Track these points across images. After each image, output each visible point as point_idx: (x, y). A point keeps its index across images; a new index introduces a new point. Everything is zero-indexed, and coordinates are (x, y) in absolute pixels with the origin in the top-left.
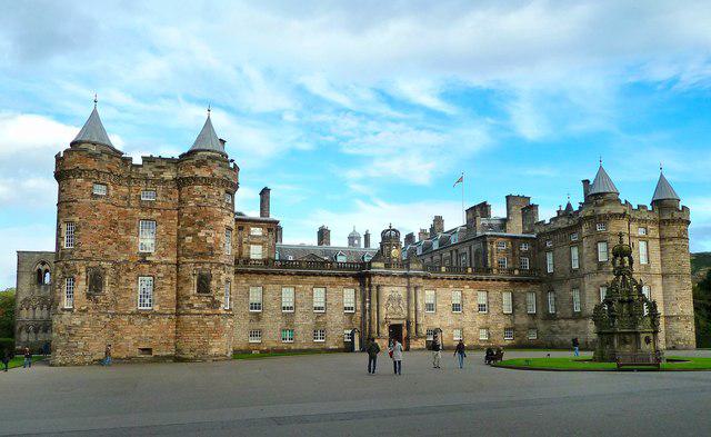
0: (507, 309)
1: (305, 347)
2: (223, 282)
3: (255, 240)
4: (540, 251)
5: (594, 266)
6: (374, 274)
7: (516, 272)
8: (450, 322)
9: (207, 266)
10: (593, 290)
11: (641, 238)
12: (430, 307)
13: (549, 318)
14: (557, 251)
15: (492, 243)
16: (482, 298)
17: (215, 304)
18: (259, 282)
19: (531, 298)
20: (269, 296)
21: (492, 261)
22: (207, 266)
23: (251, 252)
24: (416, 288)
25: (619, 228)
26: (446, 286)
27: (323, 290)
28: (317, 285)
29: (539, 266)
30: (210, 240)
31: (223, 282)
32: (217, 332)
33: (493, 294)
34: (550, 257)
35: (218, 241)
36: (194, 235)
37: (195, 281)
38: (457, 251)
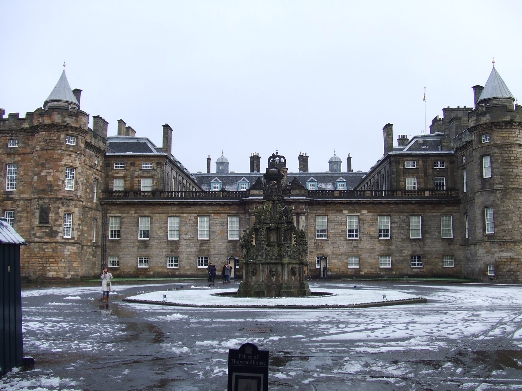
1: (189, 273)
2: (62, 214)
3: (146, 174)
4: (458, 168)
5: (478, 184)
6: (252, 202)
7: (427, 193)
9: (47, 201)
10: (478, 211)
12: (321, 233)
13: (466, 243)
14: (468, 168)
15: (398, 163)
16: (384, 223)
17: (53, 234)
18: (146, 212)
20: (157, 225)
22: (47, 201)
23: (142, 185)
24: (298, 214)
25: (504, 138)
26: (341, 212)
27: (207, 219)
29: (454, 187)
30: (50, 179)
31: (62, 214)
32: (55, 257)
33: (396, 218)
35: (57, 179)
36: (38, 174)
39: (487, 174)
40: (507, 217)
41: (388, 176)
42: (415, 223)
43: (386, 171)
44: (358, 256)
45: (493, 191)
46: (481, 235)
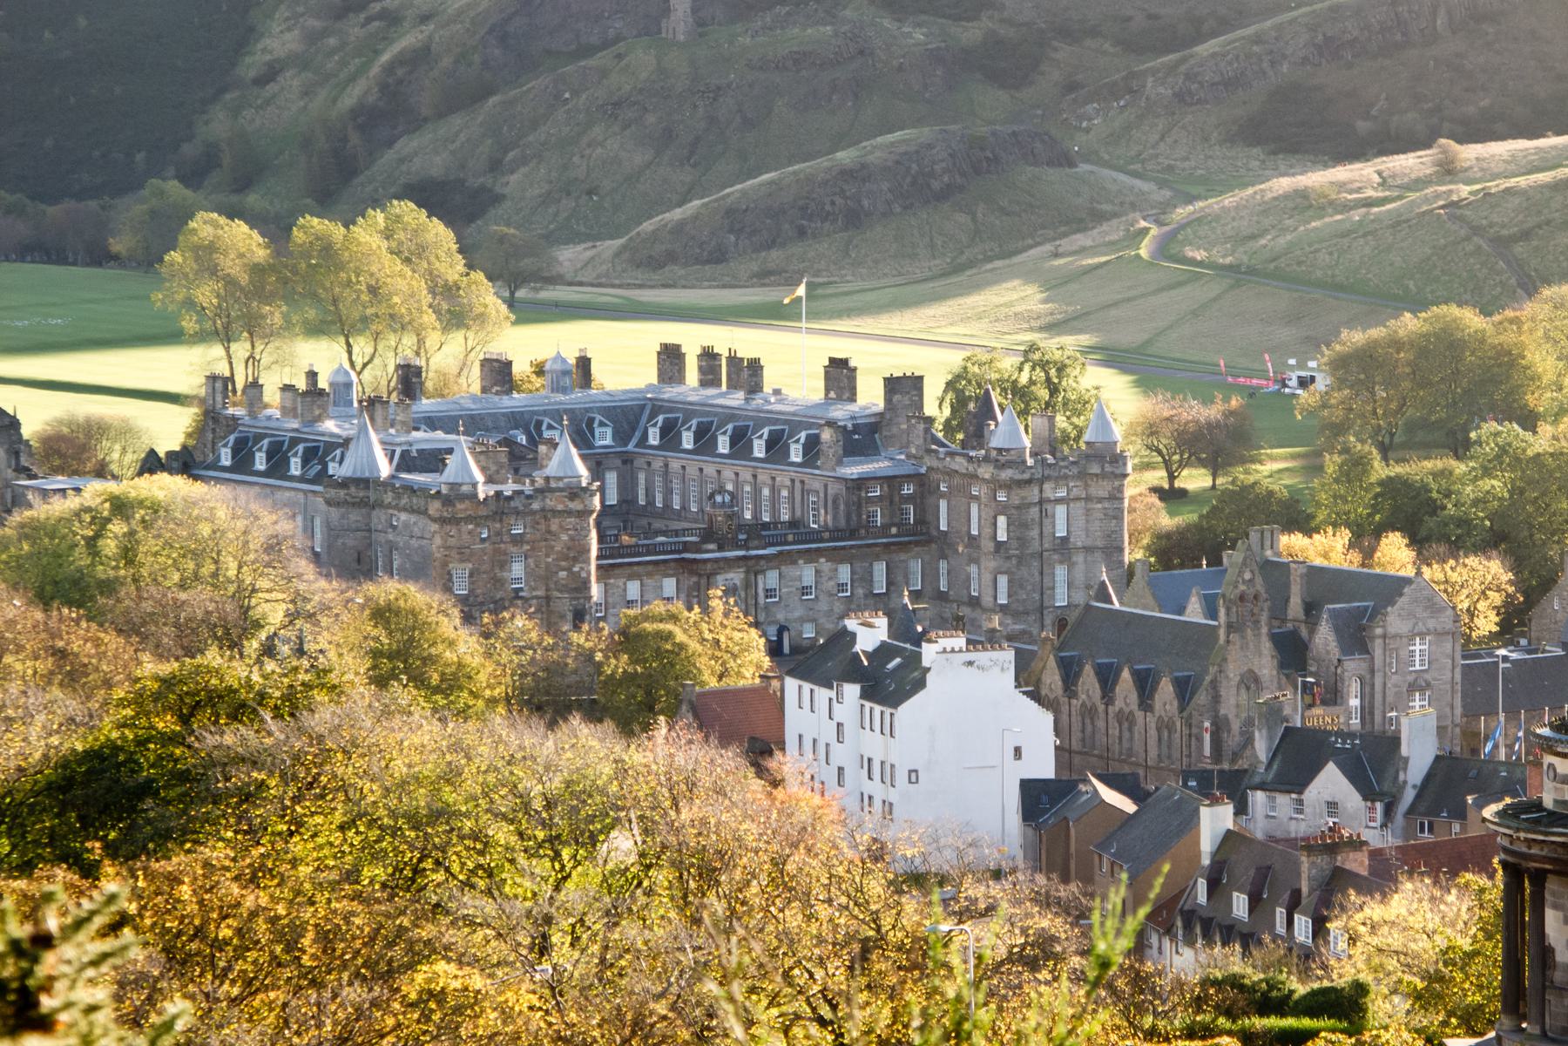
0: (880, 587)
5: (991, 546)
8: (797, 614)
11: (1059, 501)
12: (769, 593)
13: (942, 597)
15: (859, 489)
16: (844, 573)
19: (916, 567)
21: (860, 516)
25: (1023, 498)
26: (794, 562)
27: (638, 583)
28: (631, 577)
34: (943, 505)
36: (569, 569)
37: (570, 616)
38: (802, 482)
39: (1002, 536)
40: (1021, 587)
41: (834, 502)
42: (880, 569)
43: (830, 491)
44: (814, 620)
45: (1008, 558)
46: (991, 605)
